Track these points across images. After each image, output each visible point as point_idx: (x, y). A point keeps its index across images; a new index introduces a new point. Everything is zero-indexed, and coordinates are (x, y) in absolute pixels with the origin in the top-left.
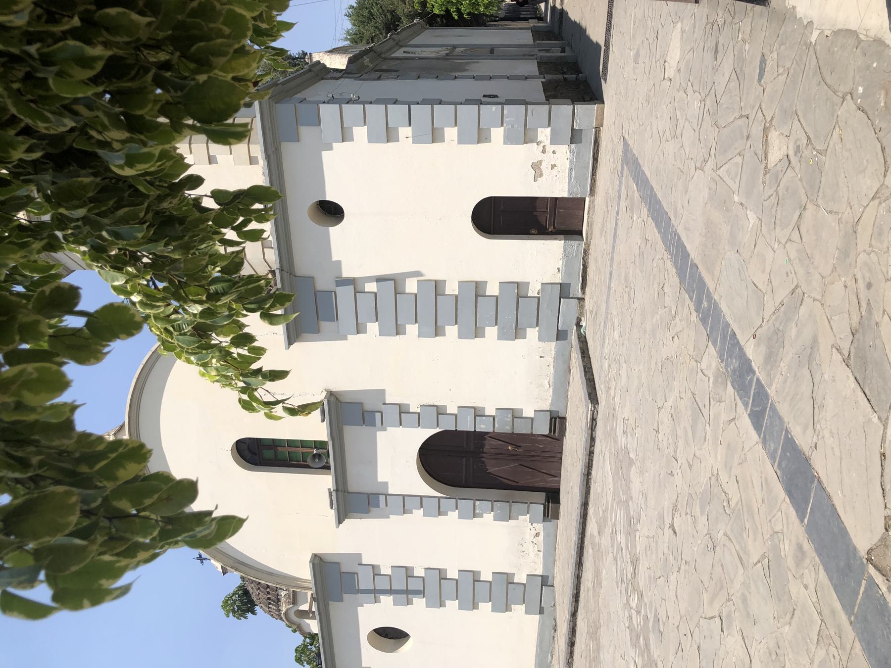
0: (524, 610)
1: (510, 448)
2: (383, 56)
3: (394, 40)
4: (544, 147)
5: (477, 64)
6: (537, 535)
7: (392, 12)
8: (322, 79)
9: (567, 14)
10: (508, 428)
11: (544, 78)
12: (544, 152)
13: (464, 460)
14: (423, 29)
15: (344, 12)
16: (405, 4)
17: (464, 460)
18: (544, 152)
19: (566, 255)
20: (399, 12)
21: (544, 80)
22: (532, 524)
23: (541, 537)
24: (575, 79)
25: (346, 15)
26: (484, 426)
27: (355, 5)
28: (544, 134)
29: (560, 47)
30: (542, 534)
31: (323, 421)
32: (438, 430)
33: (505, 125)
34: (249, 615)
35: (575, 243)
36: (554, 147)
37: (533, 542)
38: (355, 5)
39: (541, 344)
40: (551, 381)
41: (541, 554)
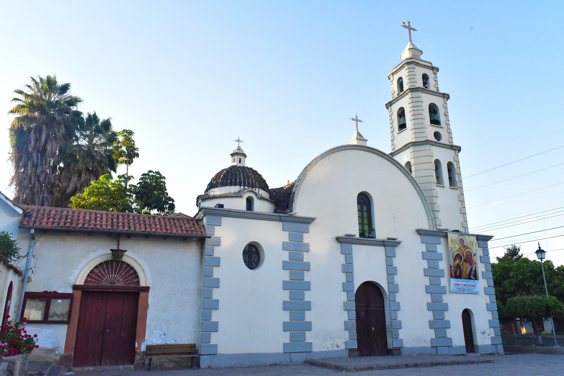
0: (286, 342)
1: (373, 328)
4: (490, 335)
6: (338, 347)
10: (394, 327)
12: (489, 335)
13: (364, 304)
17: (364, 304)
18: (489, 335)
19: (461, 347)
22: (344, 343)
23: (336, 349)
26: (393, 315)
28: (493, 335)
30: (338, 349)
31: (389, 239)
32: (387, 293)
33: (494, 320)
35: (465, 350)
36: (490, 338)
37: (333, 344)
39: (430, 339)
40: (416, 346)
41: (326, 350)
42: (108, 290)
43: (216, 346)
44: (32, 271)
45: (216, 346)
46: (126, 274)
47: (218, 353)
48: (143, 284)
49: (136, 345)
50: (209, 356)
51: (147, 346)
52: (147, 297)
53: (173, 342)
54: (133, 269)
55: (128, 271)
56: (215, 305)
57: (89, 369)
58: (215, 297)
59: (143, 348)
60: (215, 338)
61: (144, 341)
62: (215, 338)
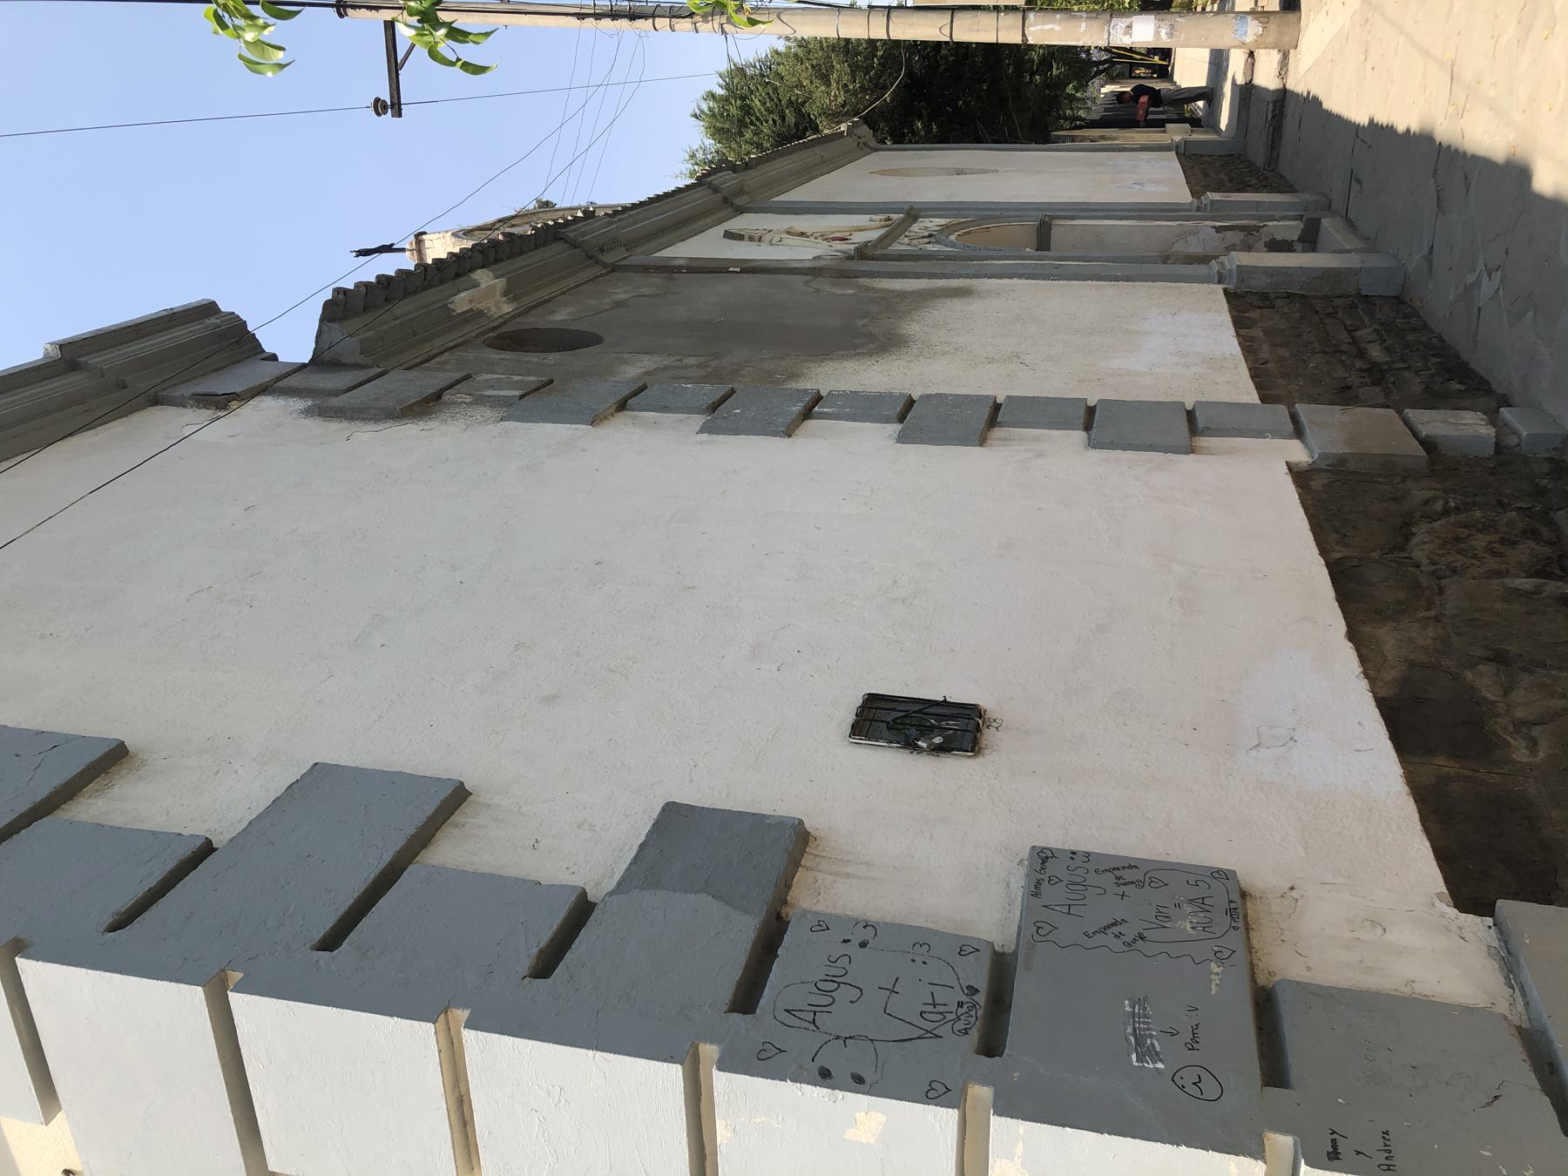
2: (609, 258)
3: (716, 191)
5: (956, 306)
7: (797, 107)
8: (156, 401)
9: (1313, 103)
11: (1299, 433)
14: (864, 149)
15: (693, 108)
16: (829, 85)
20: (812, 110)
21: (1298, 453)
24: (1489, 450)
25: (695, 116)
27: (720, 92)
29: (1300, 218)
38: (720, 92)
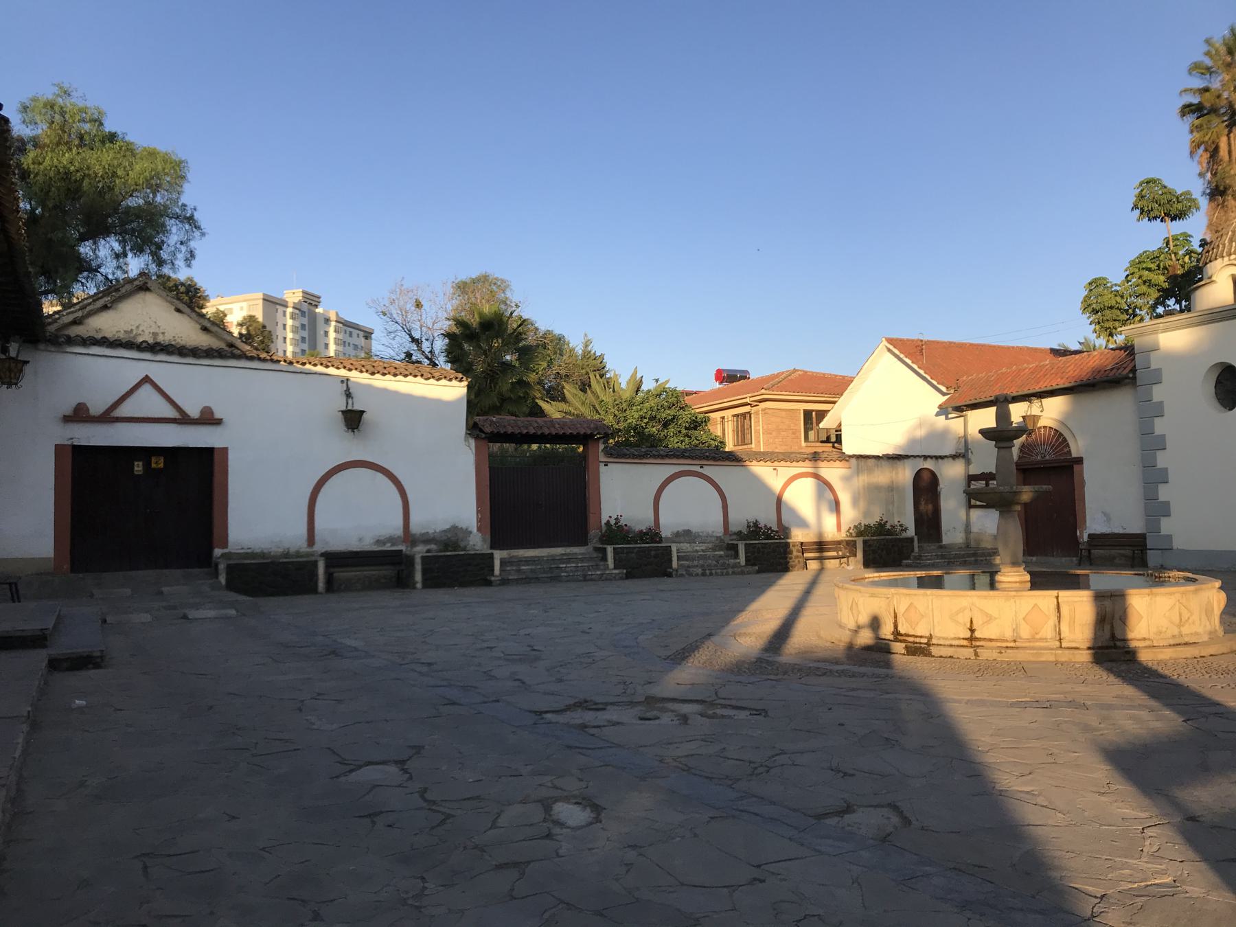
34: (1137, 212)
42: (1039, 466)
43: (1169, 537)
44: (972, 452)
45: (1169, 537)
46: (1056, 441)
47: (1175, 547)
48: (1074, 455)
49: (1078, 534)
50: (1160, 551)
51: (1089, 535)
52: (1082, 471)
53: (1121, 531)
54: (1062, 435)
55: (1057, 440)
56: (1163, 477)
57: (1032, 560)
58: (1160, 464)
59: (1085, 538)
60: (1166, 526)
61: (1086, 529)
62: (1166, 526)
